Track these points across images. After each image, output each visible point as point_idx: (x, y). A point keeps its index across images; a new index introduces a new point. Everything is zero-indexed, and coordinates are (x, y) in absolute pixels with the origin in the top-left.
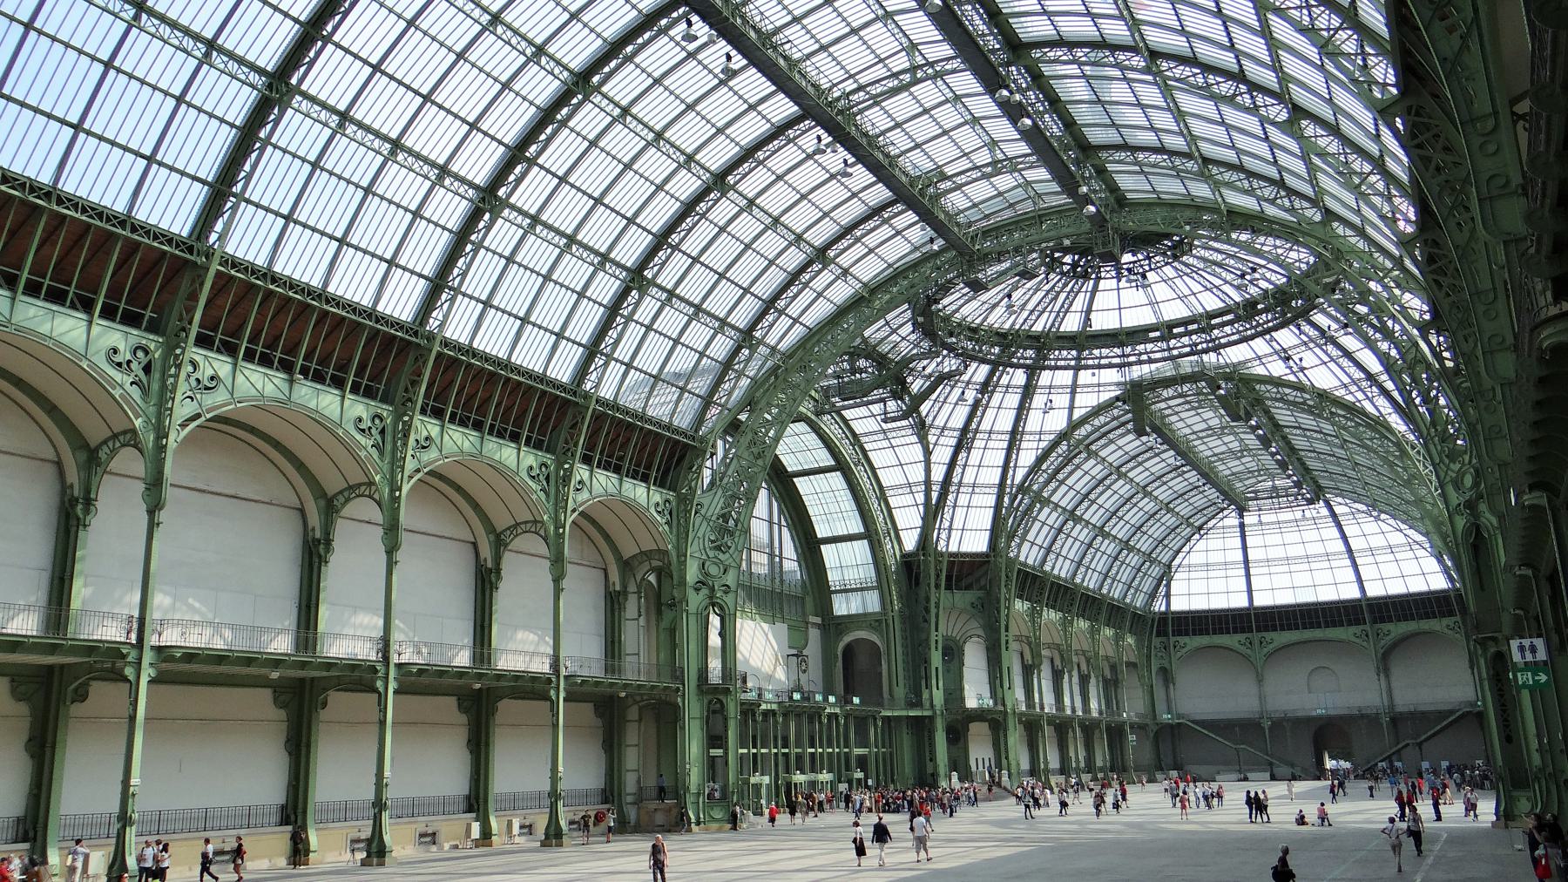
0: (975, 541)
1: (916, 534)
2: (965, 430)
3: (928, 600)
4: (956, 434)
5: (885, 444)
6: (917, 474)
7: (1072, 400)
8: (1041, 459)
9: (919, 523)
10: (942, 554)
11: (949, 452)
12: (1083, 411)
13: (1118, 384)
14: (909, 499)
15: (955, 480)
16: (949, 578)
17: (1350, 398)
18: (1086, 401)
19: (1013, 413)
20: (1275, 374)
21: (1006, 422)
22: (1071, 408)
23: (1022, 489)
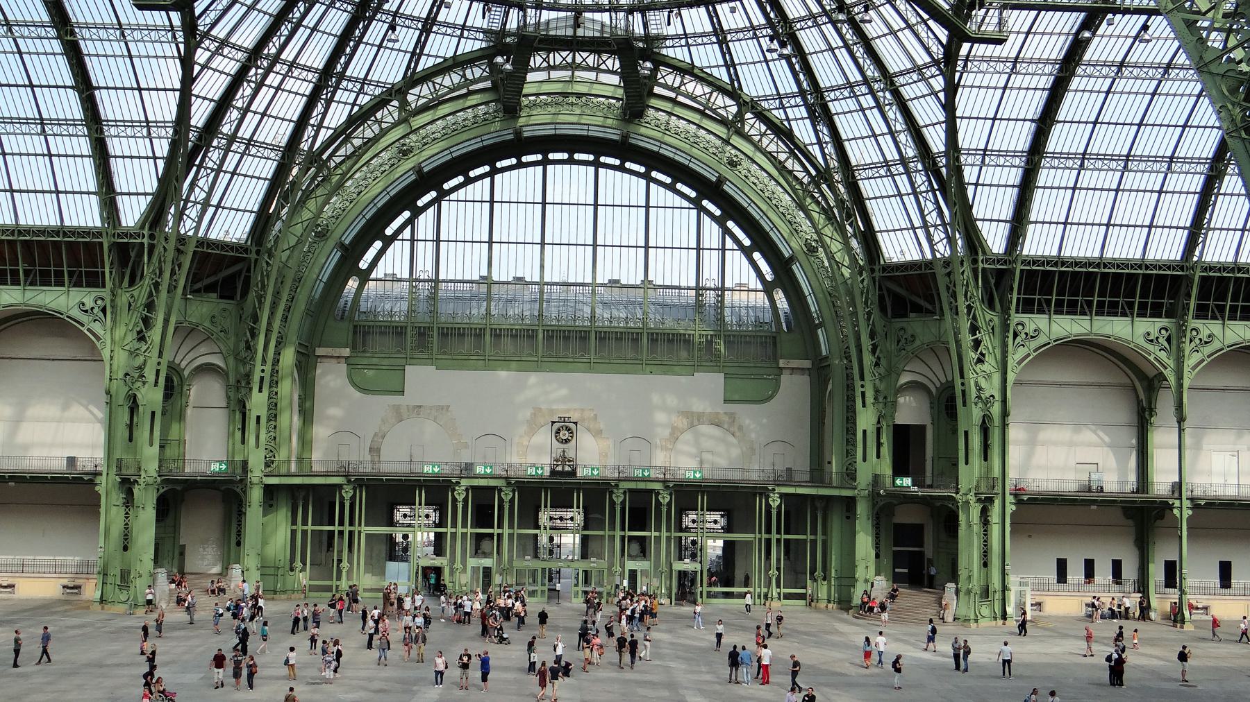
0: (232, 227)
1: (143, 203)
2: (255, 53)
3: (150, 306)
4: (240, 55)
5: (119, 48)
6: (165, 108)
7: (421, 44)
8: (354, 121)
9: (152, 185)
10: (182, 239)
11: (222, 83)
12: (431, 62)
13: (485, 31)
14: (143, 147)
15: (226, 129)
16: (194, 277)
17: (779, 114)
18: (441, 46)
19: (331, 43)
20: (697, 63)
21: (317, 54)
22: (416, 54)
23: (314, 158)
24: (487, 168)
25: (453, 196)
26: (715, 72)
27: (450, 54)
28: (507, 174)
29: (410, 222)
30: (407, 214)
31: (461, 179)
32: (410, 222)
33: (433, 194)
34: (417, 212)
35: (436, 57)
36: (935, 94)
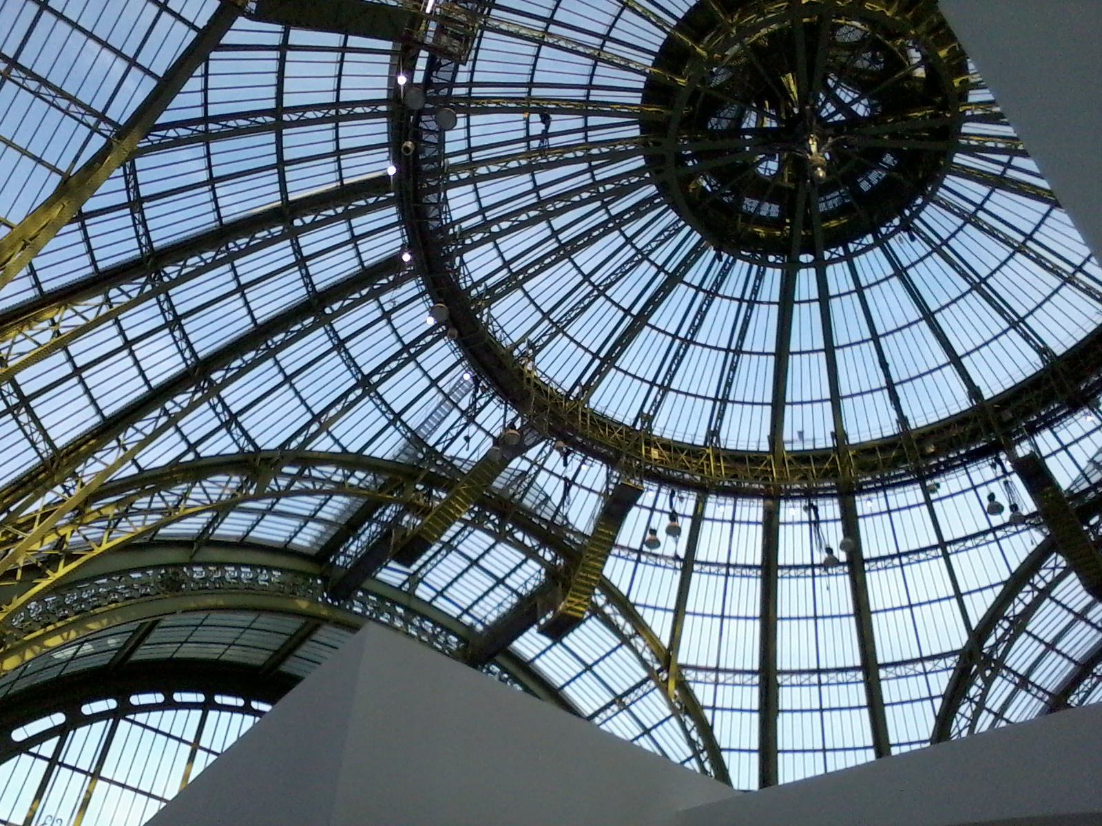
7: (344, 403)
19: (243, 325)
20: (632, 599)
24: (201, 698)
25: (141, 717)
26: (648, 616)
27: (353, 449)
28: (226, 715)
29: (61, 732)
30: (59, 718)
31: (160, 698)
32: (61, 732)
33: (112, 704)
34: (77, 720)
35: (337, 441)
36: (931, 698)
